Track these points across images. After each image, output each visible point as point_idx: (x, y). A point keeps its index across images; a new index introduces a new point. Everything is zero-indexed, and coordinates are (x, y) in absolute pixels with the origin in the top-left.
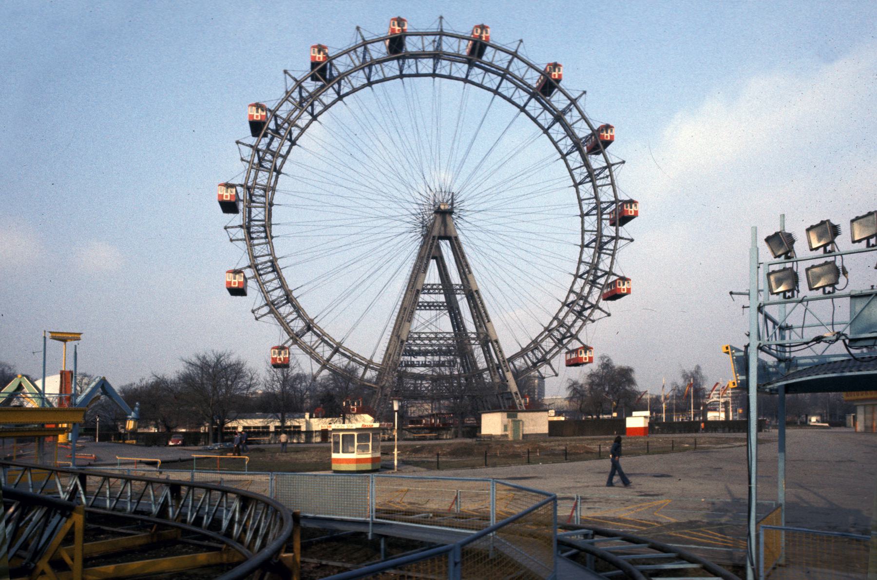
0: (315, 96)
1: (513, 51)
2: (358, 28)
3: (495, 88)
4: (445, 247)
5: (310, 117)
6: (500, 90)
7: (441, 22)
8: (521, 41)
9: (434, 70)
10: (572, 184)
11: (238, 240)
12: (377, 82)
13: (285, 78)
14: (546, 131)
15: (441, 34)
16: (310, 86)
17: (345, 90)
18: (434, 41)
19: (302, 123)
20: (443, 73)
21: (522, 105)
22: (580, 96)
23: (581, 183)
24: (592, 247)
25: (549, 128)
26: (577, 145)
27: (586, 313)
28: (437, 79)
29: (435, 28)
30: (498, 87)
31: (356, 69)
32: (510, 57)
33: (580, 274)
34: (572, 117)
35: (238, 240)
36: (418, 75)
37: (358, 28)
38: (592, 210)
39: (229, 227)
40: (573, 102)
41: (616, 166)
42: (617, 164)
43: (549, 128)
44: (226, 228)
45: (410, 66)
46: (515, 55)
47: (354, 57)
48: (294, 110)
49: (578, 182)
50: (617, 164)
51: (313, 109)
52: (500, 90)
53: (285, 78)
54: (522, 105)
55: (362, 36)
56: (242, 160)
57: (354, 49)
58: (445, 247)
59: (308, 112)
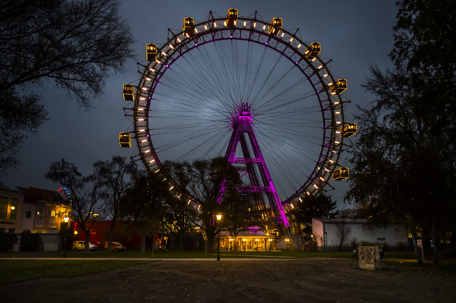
1: (293, 34)
2: (211, 12)
3: (282, 51)
4: (246, 135)
5: (179, 54)
7: (256, 14)
8: (298, 29)
10: (321, 109)
11: (129, 115)
14: (308, 78)
20: (254, 39)
22: (328, 62)
23: (325, 110)
25: (310, 77)
28: (251, 42)
30: (284, 51)
35: (129, 115)
36: (240, 39)
37: (211, 12)
38: (330, 126)
39: (126, 109)
41: (345, 103)
42: (346, 102)
43: (310, 77)
44: (124, 109)
49: (324, 109)
50: (346, 102)
51: (181, 50)
52: (285, 53)
55: (212, 16)
56: (139, 72)
58: (246, 135)
59: (179, 51)
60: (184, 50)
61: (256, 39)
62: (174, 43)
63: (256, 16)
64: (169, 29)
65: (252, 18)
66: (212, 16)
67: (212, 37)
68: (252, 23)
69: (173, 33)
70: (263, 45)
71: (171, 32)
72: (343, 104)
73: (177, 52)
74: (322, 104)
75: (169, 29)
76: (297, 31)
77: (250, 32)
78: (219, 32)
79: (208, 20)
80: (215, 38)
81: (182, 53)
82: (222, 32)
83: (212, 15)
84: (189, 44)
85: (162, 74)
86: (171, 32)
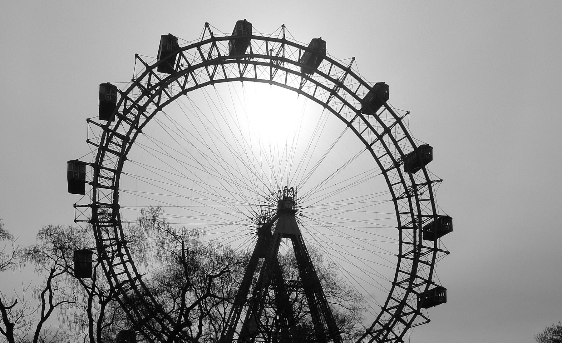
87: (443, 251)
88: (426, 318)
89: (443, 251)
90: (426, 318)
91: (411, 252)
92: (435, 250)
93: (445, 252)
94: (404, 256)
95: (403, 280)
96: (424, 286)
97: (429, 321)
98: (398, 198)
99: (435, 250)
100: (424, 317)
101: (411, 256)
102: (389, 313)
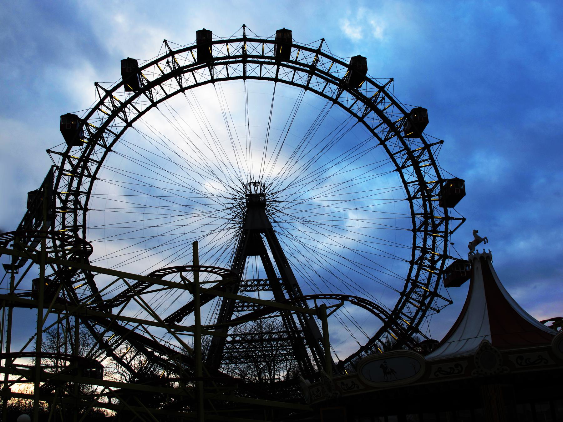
0: (85, 159)
1: (242, 37)
3: (242, 74)
5: (90, 179)
6: (247, 74)
8: (244, 26)
9: (181, 86)
12: (135, 120)
13: (51, 157)
15: (172, 54)
16: (76, 152)
17: (109, 141)
18: (168, 62)
19: (85, 187)
21: (274, 76)
24: (408, 166)
26: (343, 85)
27: (442, 228)
29: (164, 51)
30: (244, 73)
31: (111, 118)
32: (242, 43)
33: (412, 196)
34: (324, 64)
40: (318, 52)
41: (387, 86)
42: (387, 84)
43: (308, 83)
45: (157, 93)
46: (245, 39)
47: (104, 109)
48: (72, 180)
53: (51, 157)
54: (274, 76)
55: (103, 89)
57: (102, 102)
59: (85, 176)
60: (93, 167)
61: (192, 82)
62: (71, 167)
63: (169, 48)
64: (48, 151)
65: (165, 54)
66: (103, 89)
67: (123, 121)
68: (169, 64)
69: (58, 153)
70: (208, 84)
71: (54, 152)
72: (386, 89)
73: (84, 178)
74: (354, 111)
75: (48, 151)
76: (244, 28)
77: (176, 78)
78: (128, 106)
79: (99, 100)
80: (129, 121)
81: (92, 174)
82: (134, 104)
83: (101, 87)
84: (95, 155)
85: (84, 227)
86: (54, 152)
87: (436, 144)
88: (460, 219)
89: (436, 144)
90: (460, 219)
91: (407, 160)
92: (427, 147)
93: (438, 143)
94: (403, 167)
95: (416, 191)
96: (439, 187)
97: (464, 220)
98: (363, 117)
99: (427, 147)
100: (456, 219)
101: (409, 163)
102: (422, 231)
